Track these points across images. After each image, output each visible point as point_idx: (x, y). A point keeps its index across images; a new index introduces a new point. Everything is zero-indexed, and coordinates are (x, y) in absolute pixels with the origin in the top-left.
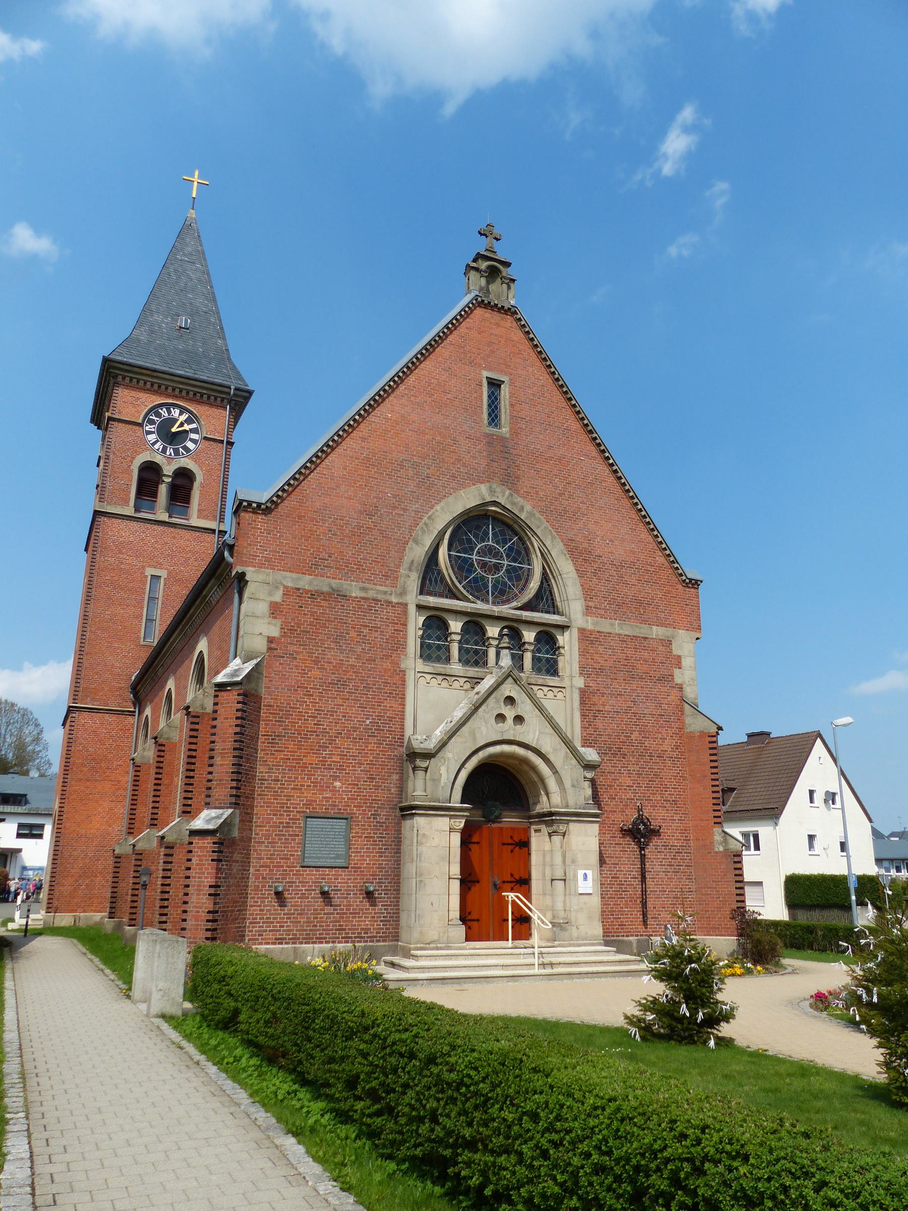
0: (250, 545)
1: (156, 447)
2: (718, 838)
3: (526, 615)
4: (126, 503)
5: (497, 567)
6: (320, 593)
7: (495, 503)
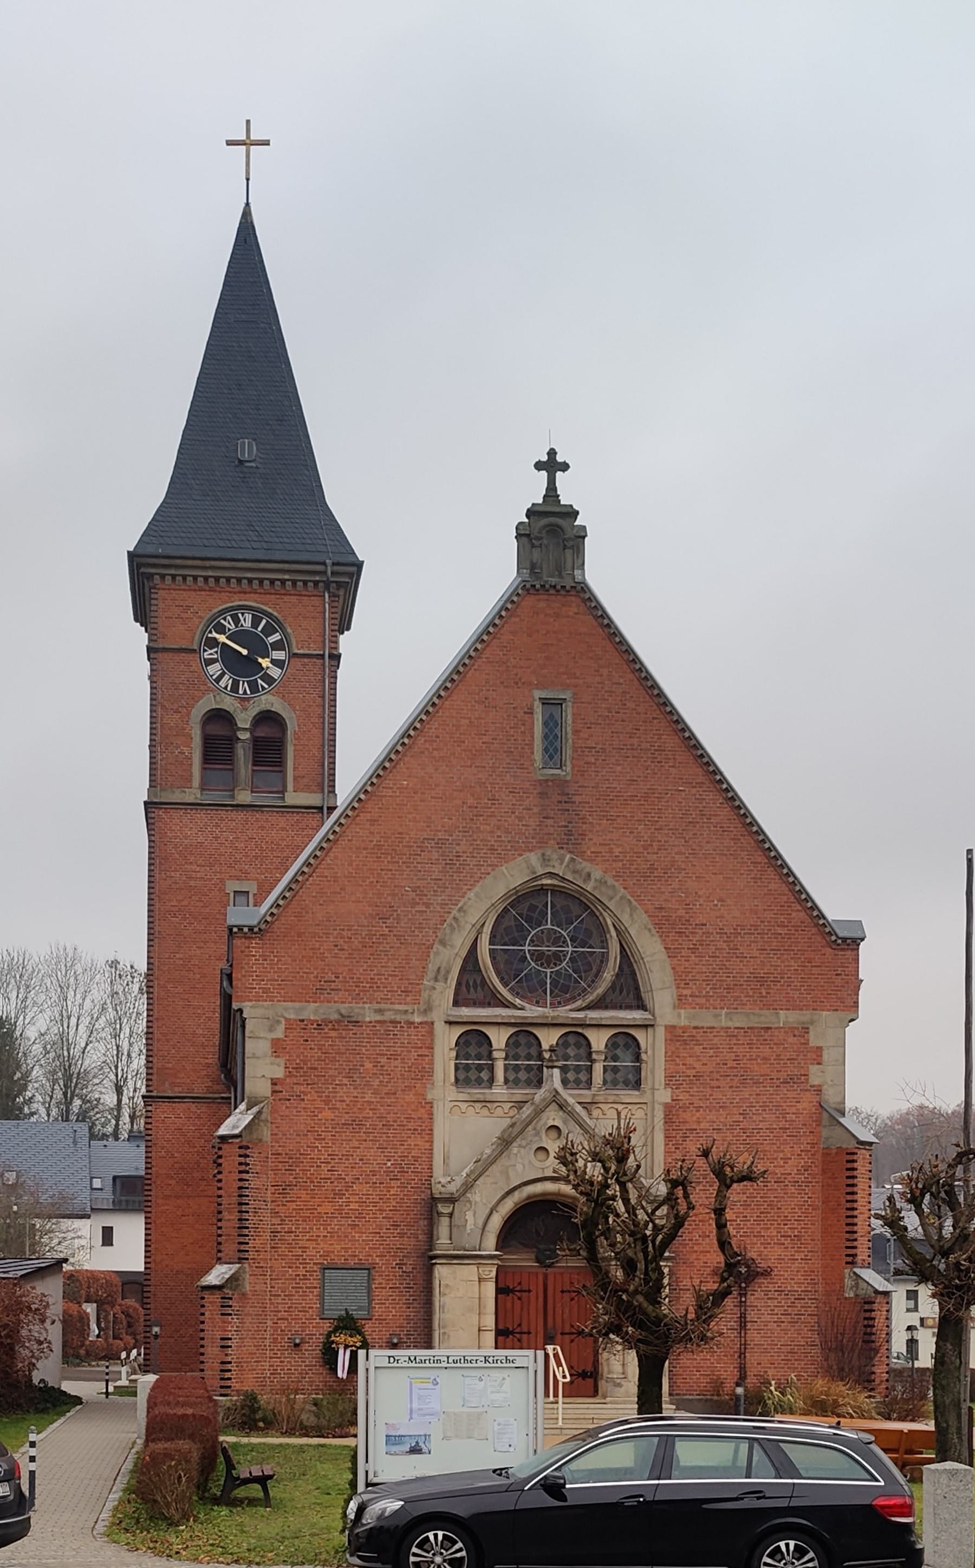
0: (245, 976)
1: (222, 683)
2: (848, 1282)
3: (594, 1015)
4: (187, 781)
5: (557, 958)
6: (327, 1022)
7: (551, 875)
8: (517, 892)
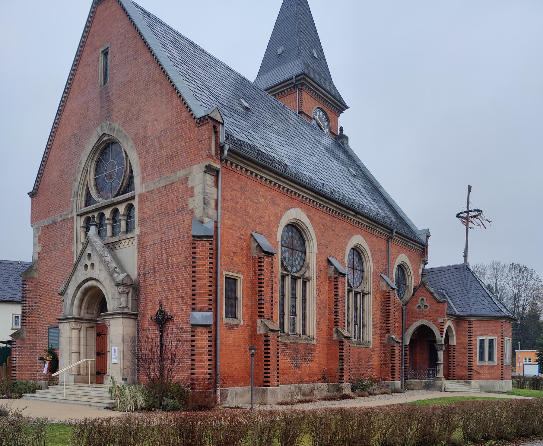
8: (98, 148)
